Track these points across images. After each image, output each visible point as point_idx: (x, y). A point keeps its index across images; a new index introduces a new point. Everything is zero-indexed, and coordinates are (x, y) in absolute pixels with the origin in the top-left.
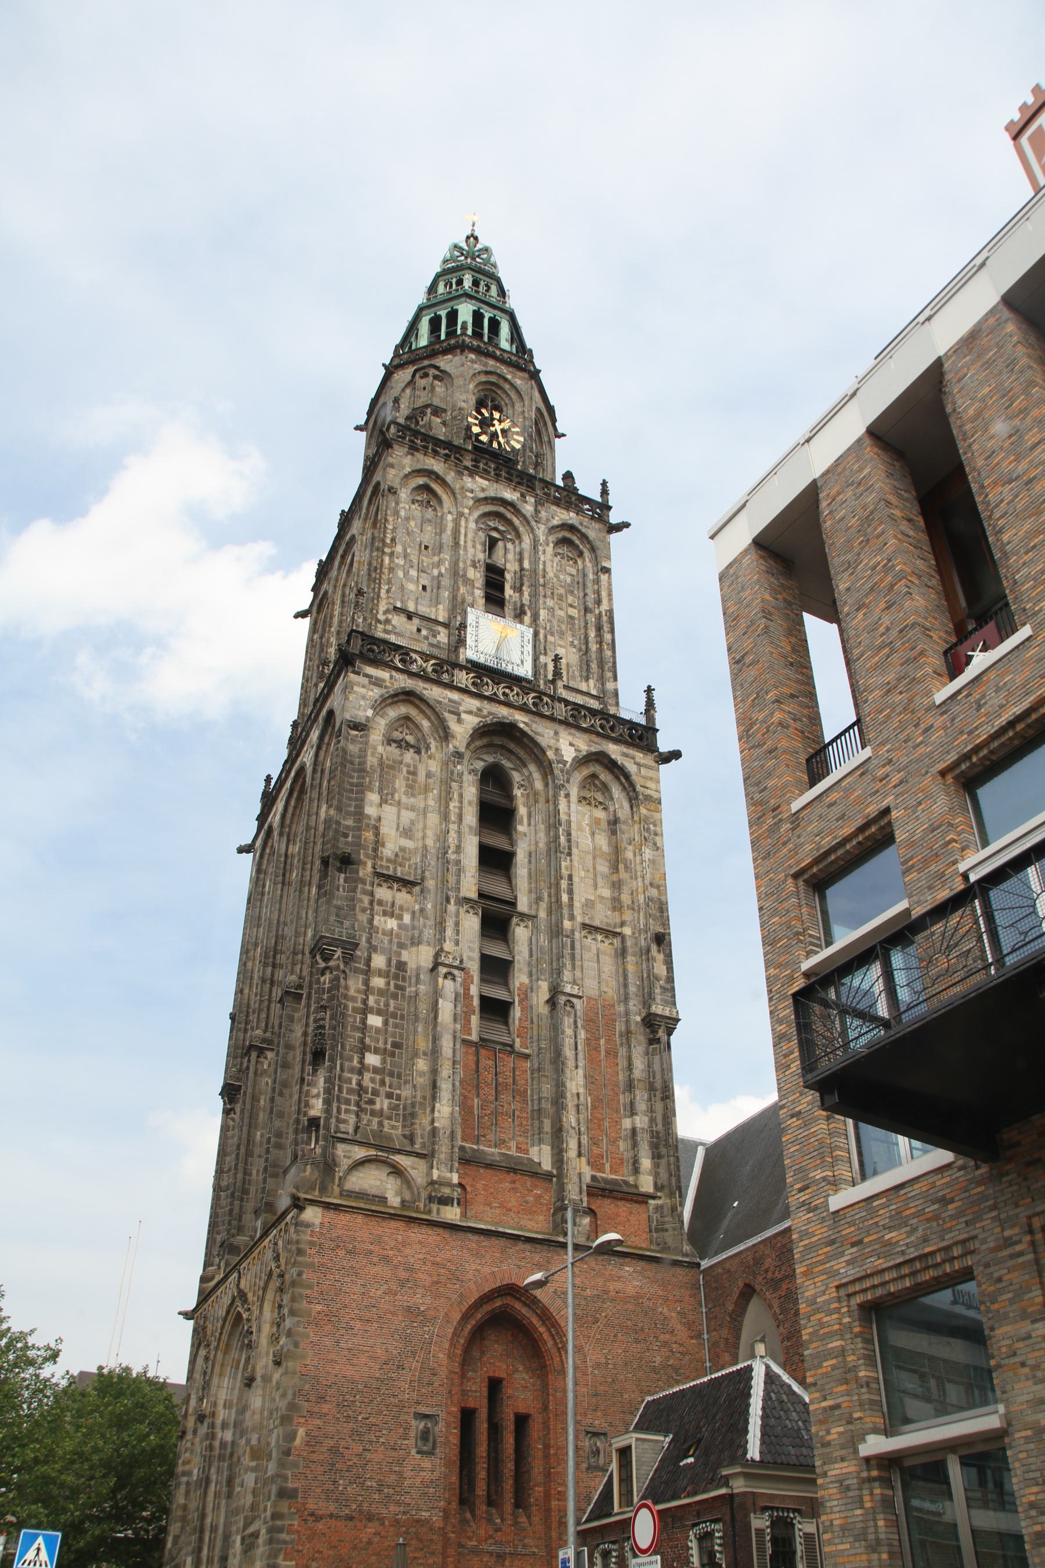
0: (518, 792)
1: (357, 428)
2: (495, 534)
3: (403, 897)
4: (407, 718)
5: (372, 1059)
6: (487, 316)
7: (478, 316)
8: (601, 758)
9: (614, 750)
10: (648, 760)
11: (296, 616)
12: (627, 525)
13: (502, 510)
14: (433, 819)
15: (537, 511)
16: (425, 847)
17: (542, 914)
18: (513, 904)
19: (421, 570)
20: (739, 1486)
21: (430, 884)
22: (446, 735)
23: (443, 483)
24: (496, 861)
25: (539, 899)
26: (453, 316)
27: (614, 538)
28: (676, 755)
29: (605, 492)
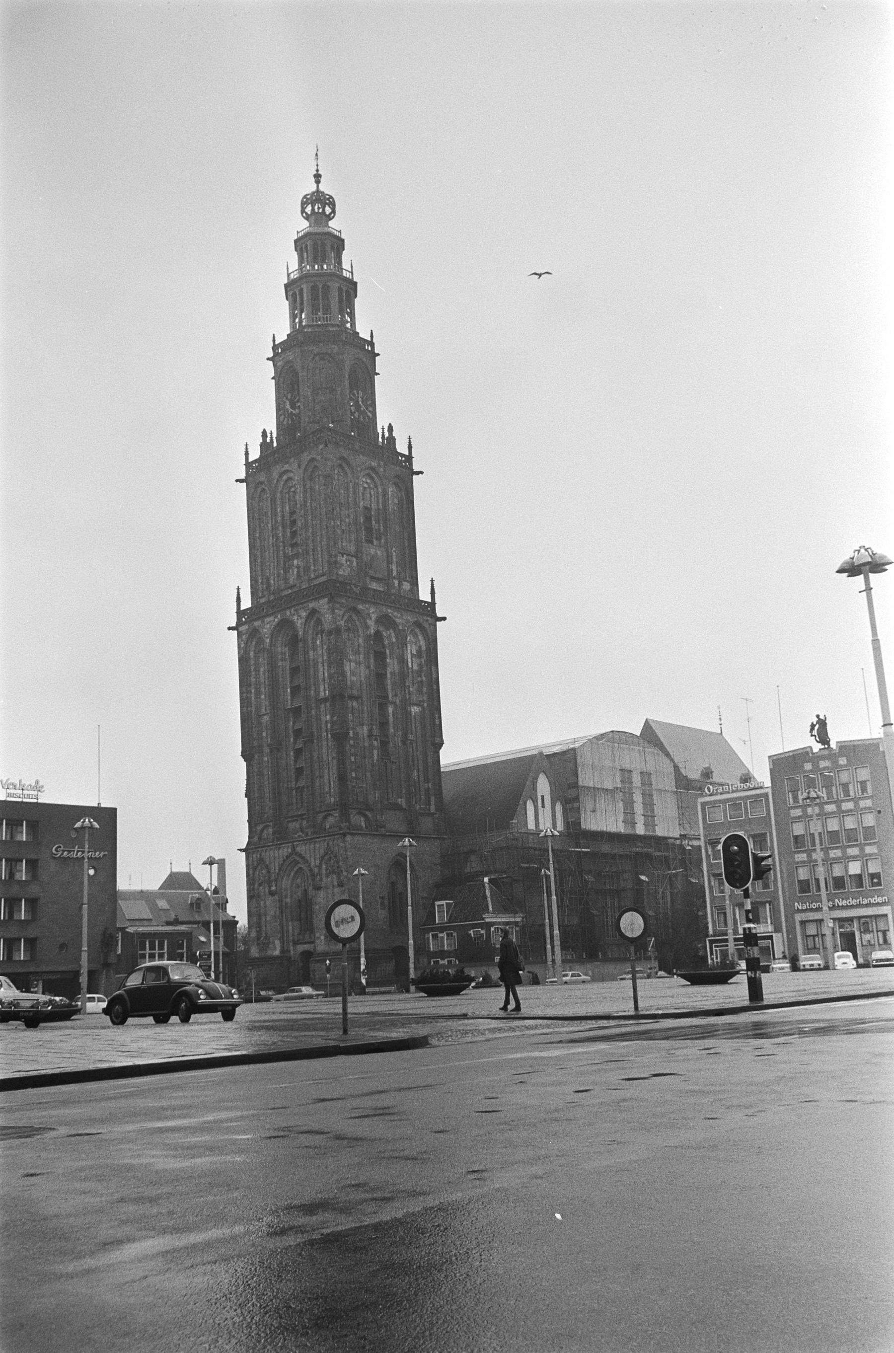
0: (386, 642)
1: (268, 359)
2: (366, 485)
3: (355, 704)
4: (351, 616)
5: (354, 775)
6: (344, 289)
7: (340, 289)
8: (418, 624)
9: (421, 619)
10: (431, 620)
11: (237, 481)
12: (422, 473)
13: (371, 473)
14: (362, 667)
15: (385, 471)
16: (361, 681)
17: (398, 702)
18: (386, 697)
19: (341, 521)
20: (487, 920)
21: (365, 699)
22: (367, 627)
23: (348, 464)
24: (380, 676)
25: (396, 695)
26: (326, 288)
27: (414, 477)
28: (444, 619)
29: (410, 447)
